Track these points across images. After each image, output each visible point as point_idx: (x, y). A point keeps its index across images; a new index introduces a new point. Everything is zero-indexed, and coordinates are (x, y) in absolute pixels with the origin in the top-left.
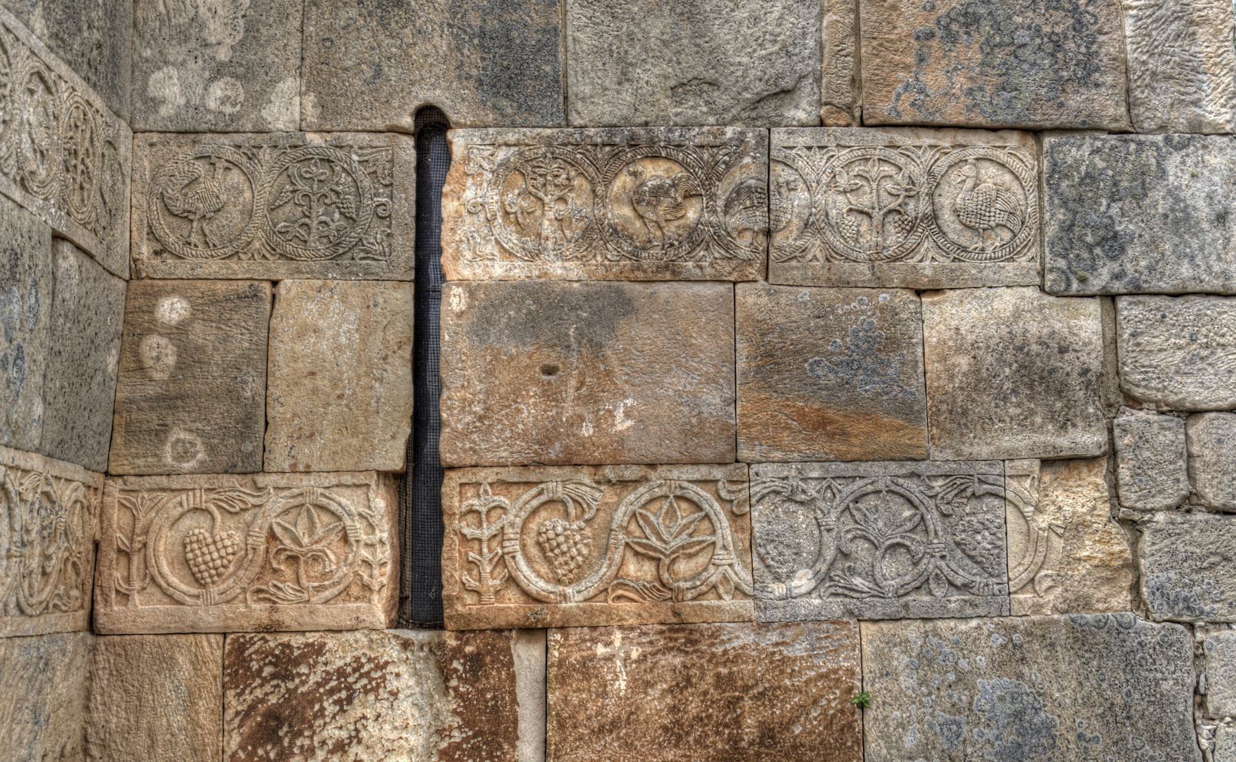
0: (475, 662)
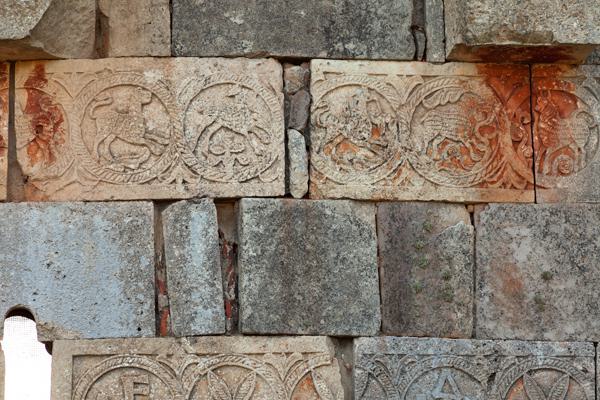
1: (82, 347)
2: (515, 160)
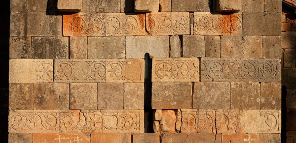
1: (157, 59)
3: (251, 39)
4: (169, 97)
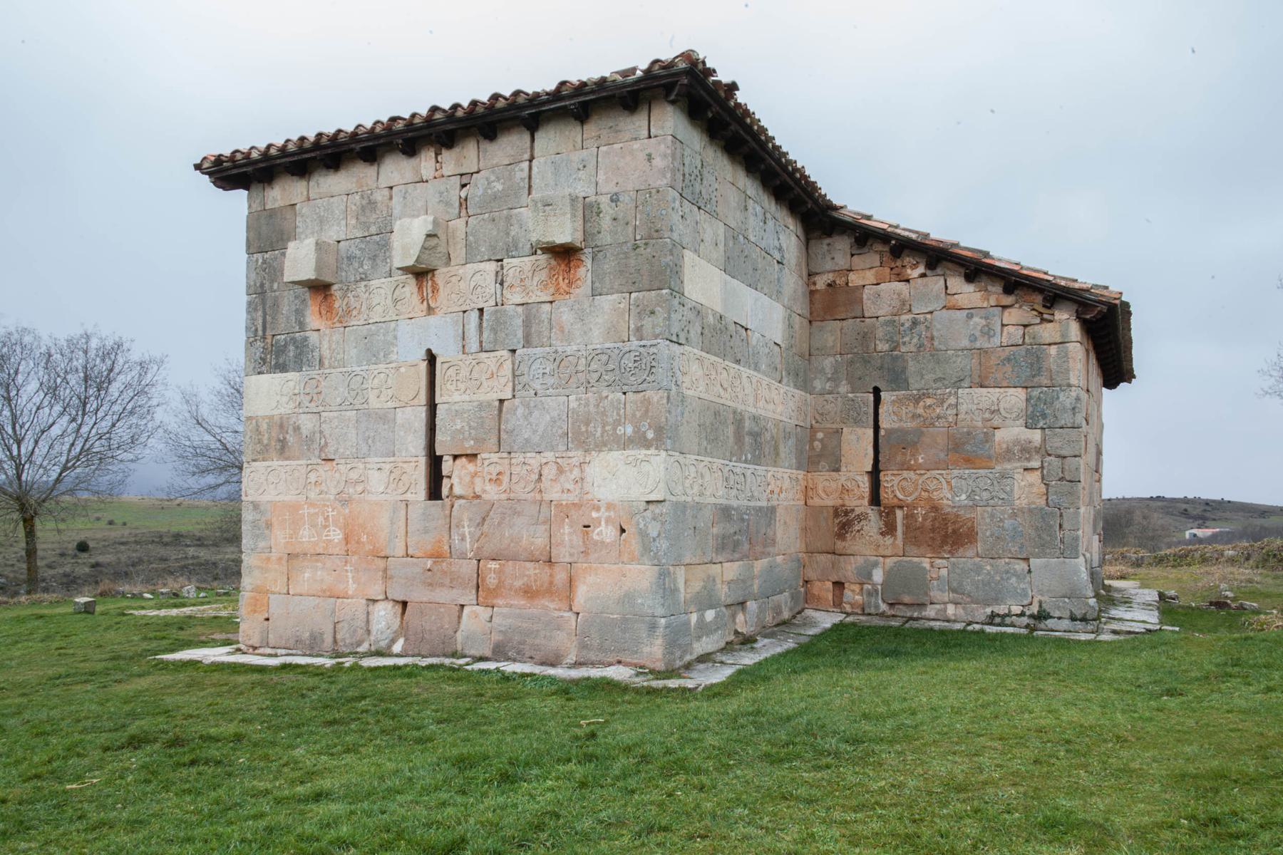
0: (888, 514)
2: (563, 285)
3: (608, 302)
4: (461, 431)
